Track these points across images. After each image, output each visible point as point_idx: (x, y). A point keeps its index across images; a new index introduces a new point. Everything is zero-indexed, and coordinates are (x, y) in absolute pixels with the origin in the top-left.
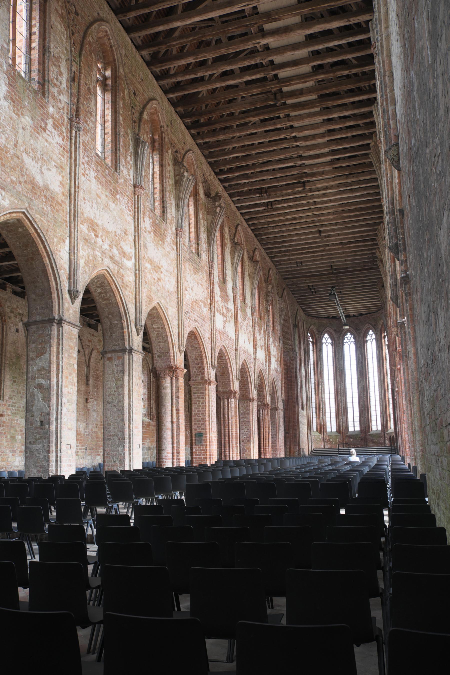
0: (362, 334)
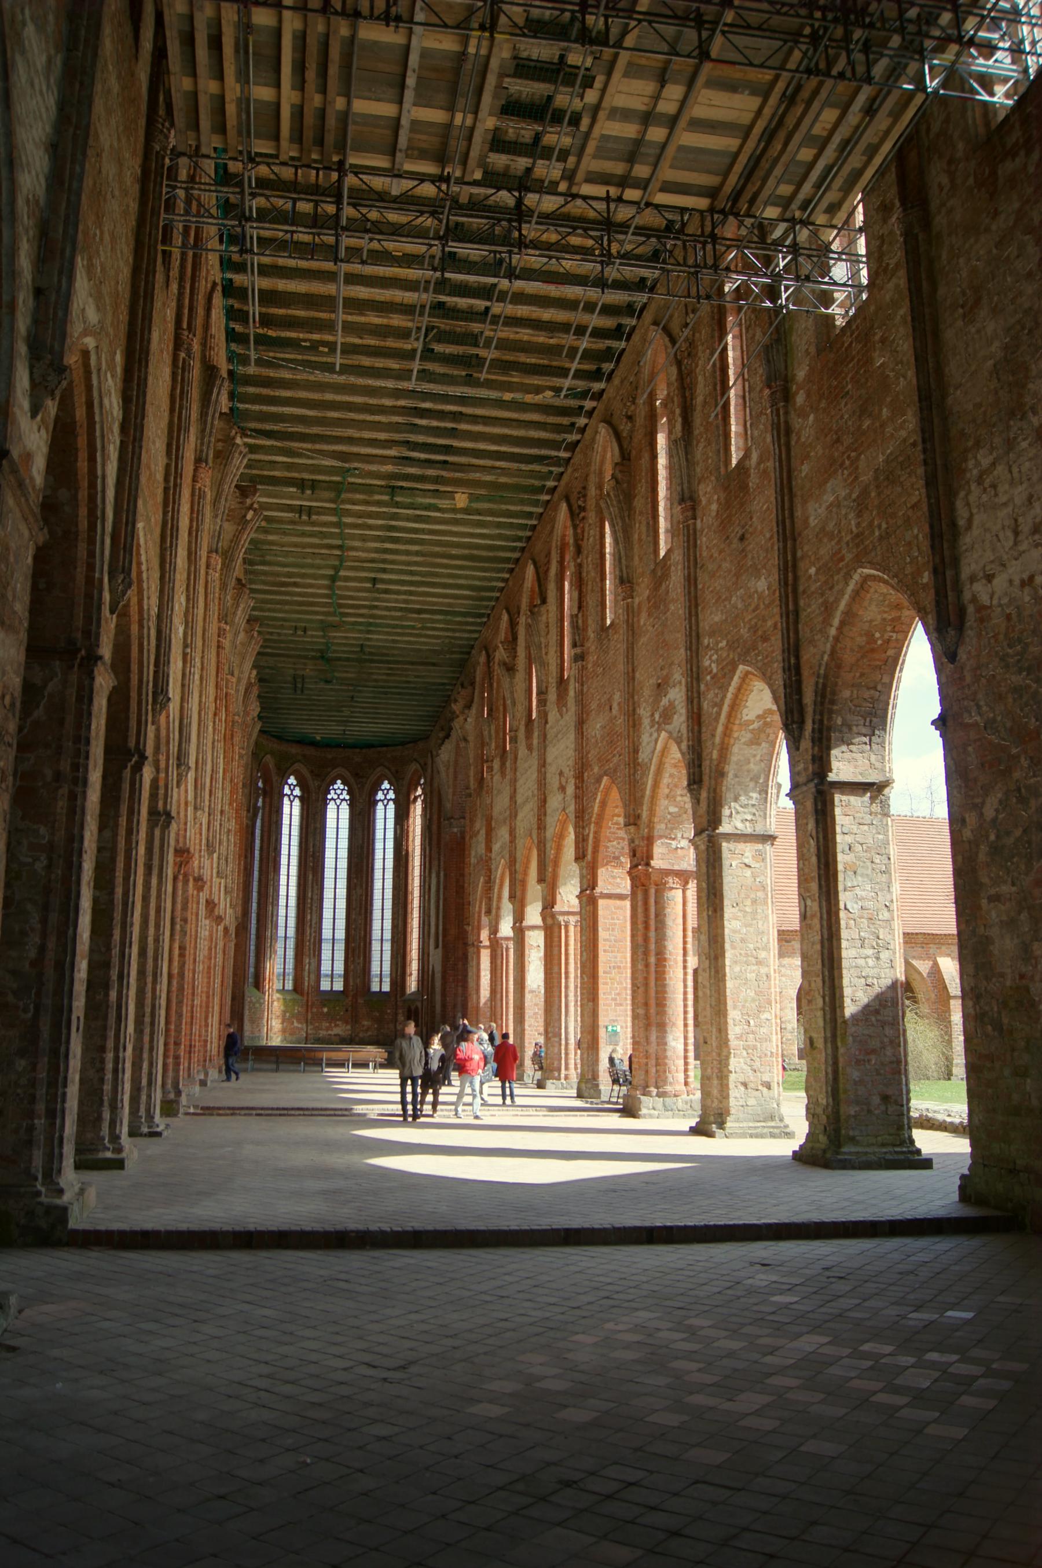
0: (368, 786)
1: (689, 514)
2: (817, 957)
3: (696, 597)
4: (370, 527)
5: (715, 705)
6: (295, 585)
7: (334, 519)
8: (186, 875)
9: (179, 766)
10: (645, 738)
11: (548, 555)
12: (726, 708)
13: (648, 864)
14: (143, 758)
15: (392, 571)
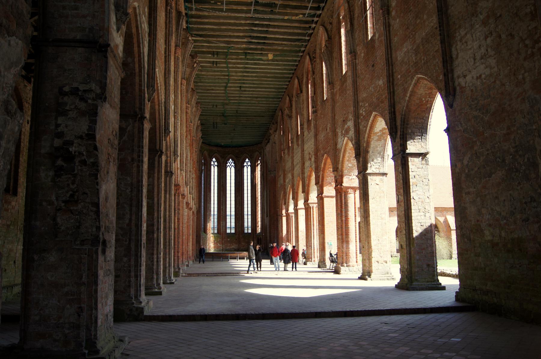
1: (353, 58)
2: (403, 216)
3: (357, 88)
4: (238, 68)
5: (364, 127)
6: (212, 90)
7: (225, 65)
8: (178, 194)
9: (174, 155)
10: (339, 140)
11: (303, 75)
12: (368, 128)
13: (341, 185)
14: (162, 152)
15: (247, 83)
